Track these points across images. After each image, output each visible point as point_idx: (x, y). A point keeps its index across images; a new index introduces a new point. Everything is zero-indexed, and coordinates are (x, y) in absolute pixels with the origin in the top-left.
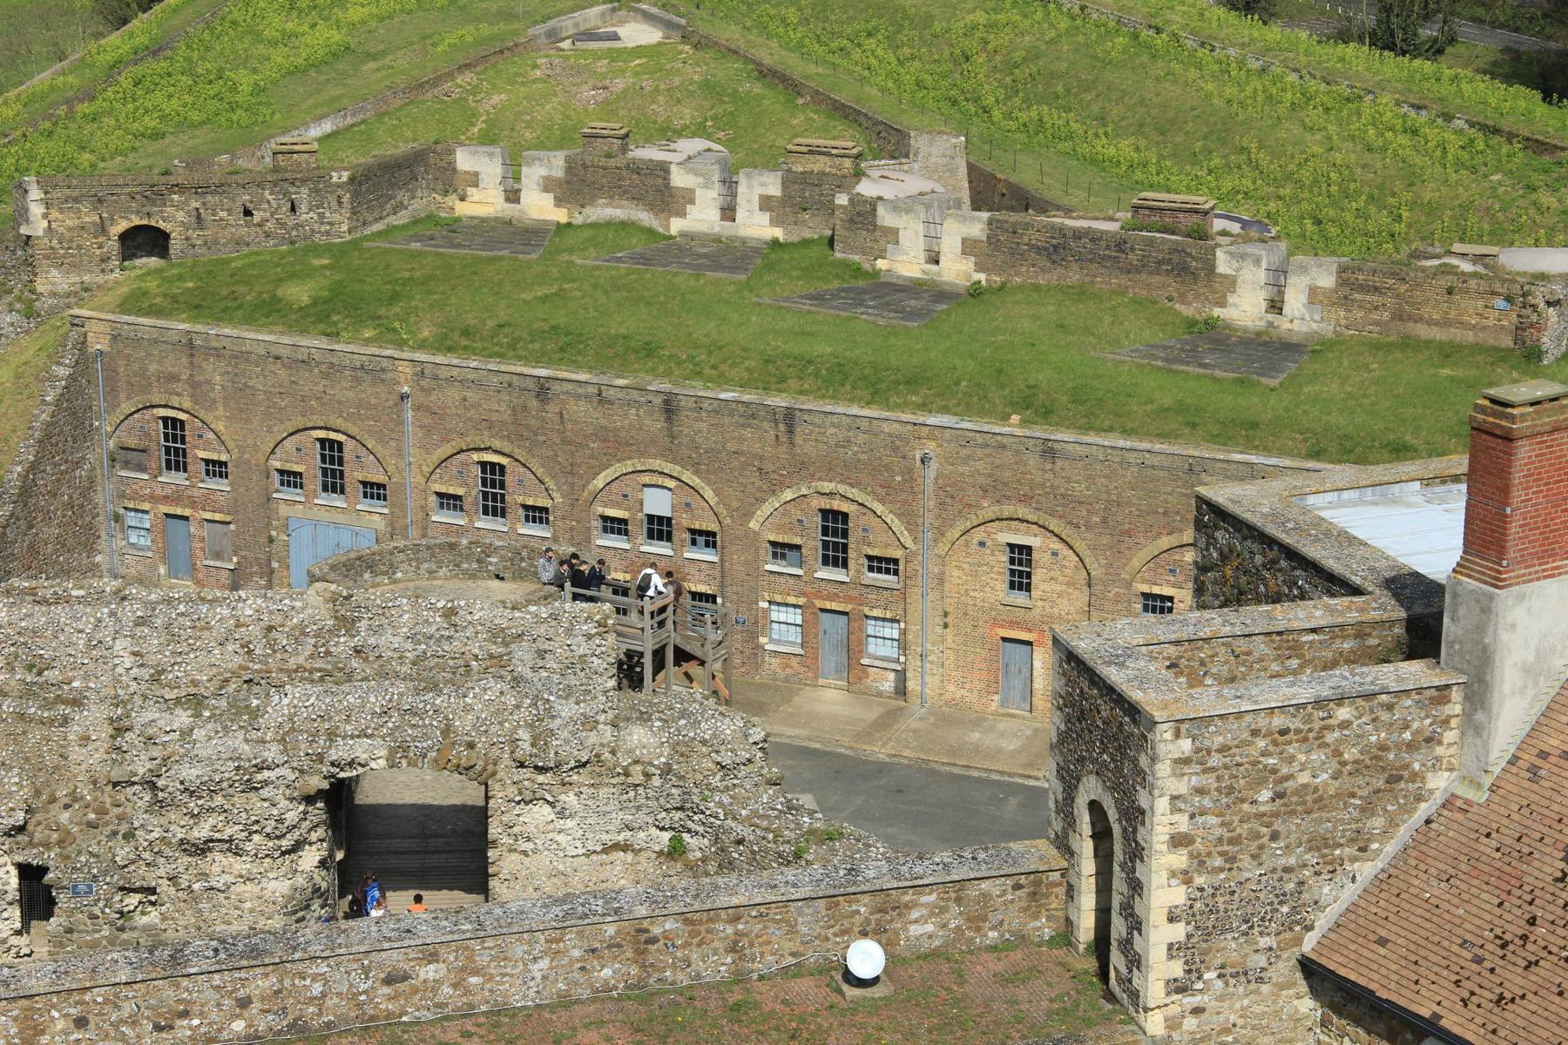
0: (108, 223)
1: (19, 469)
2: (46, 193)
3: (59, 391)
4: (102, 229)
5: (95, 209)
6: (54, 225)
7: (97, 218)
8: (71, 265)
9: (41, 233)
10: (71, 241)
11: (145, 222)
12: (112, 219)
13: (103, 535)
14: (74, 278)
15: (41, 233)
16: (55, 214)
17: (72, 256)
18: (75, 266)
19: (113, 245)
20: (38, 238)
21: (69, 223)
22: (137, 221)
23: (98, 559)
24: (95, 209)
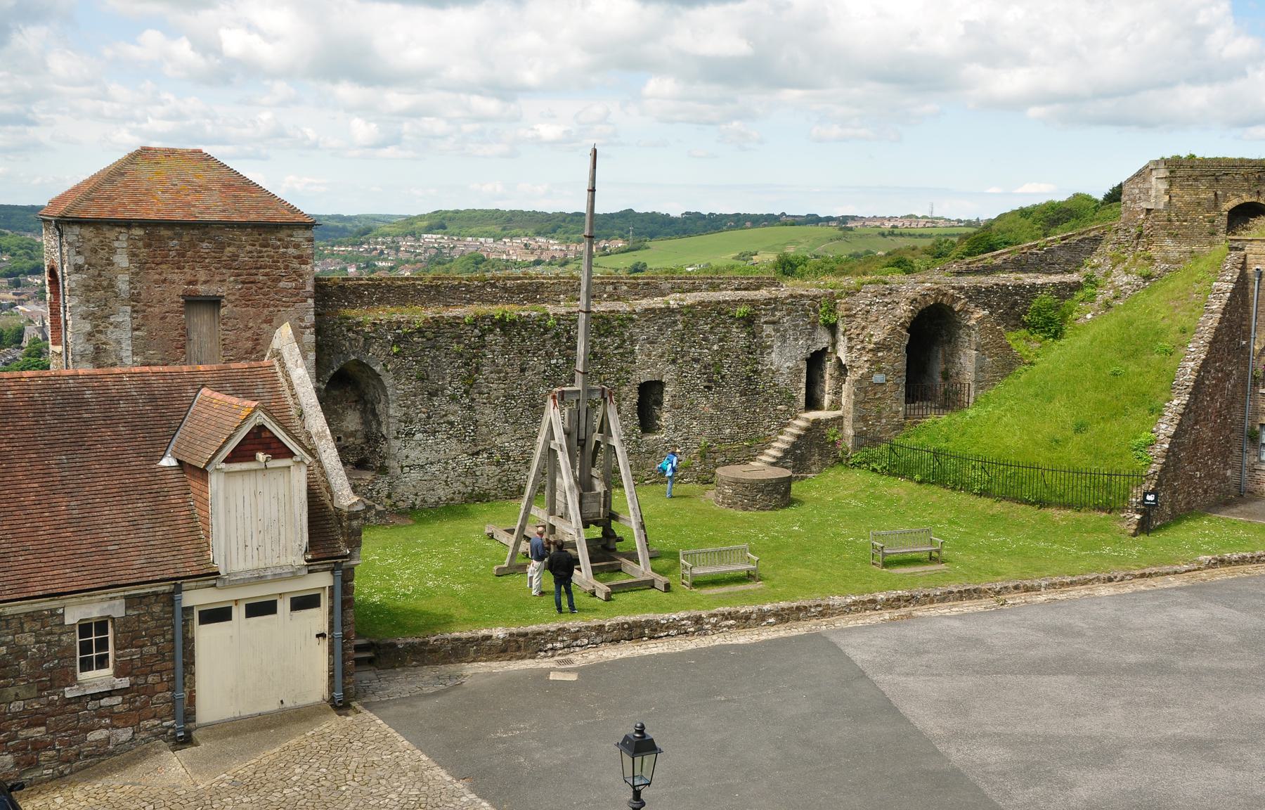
0: (1221, 199)
1: (1192, 364)
2: (1171, 172)
3: (1224, 302)
4: (1216, 206)
5: (1211, 186)
6: (1174, 200)
7: (1212, 195)
8: (1185, 236)
9: (1161, 206)
10: (1187, 214)
11: (1254, 199)
12: (1225, 196)
13: (1236, 451)
14: (1184, 248)
15: (1161, 206)
16: (1176, 190)
17: (1186, 227)
18: (1188, 238)
19: (1222, 221)
20: (1158, 211)
21: (1187, 198)
22: (1247, 198)
23: (1229, 473)
24: (1211, 186)
